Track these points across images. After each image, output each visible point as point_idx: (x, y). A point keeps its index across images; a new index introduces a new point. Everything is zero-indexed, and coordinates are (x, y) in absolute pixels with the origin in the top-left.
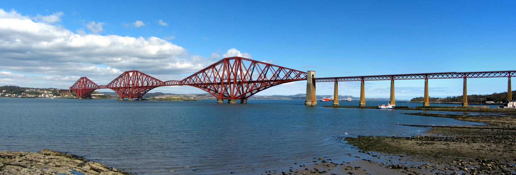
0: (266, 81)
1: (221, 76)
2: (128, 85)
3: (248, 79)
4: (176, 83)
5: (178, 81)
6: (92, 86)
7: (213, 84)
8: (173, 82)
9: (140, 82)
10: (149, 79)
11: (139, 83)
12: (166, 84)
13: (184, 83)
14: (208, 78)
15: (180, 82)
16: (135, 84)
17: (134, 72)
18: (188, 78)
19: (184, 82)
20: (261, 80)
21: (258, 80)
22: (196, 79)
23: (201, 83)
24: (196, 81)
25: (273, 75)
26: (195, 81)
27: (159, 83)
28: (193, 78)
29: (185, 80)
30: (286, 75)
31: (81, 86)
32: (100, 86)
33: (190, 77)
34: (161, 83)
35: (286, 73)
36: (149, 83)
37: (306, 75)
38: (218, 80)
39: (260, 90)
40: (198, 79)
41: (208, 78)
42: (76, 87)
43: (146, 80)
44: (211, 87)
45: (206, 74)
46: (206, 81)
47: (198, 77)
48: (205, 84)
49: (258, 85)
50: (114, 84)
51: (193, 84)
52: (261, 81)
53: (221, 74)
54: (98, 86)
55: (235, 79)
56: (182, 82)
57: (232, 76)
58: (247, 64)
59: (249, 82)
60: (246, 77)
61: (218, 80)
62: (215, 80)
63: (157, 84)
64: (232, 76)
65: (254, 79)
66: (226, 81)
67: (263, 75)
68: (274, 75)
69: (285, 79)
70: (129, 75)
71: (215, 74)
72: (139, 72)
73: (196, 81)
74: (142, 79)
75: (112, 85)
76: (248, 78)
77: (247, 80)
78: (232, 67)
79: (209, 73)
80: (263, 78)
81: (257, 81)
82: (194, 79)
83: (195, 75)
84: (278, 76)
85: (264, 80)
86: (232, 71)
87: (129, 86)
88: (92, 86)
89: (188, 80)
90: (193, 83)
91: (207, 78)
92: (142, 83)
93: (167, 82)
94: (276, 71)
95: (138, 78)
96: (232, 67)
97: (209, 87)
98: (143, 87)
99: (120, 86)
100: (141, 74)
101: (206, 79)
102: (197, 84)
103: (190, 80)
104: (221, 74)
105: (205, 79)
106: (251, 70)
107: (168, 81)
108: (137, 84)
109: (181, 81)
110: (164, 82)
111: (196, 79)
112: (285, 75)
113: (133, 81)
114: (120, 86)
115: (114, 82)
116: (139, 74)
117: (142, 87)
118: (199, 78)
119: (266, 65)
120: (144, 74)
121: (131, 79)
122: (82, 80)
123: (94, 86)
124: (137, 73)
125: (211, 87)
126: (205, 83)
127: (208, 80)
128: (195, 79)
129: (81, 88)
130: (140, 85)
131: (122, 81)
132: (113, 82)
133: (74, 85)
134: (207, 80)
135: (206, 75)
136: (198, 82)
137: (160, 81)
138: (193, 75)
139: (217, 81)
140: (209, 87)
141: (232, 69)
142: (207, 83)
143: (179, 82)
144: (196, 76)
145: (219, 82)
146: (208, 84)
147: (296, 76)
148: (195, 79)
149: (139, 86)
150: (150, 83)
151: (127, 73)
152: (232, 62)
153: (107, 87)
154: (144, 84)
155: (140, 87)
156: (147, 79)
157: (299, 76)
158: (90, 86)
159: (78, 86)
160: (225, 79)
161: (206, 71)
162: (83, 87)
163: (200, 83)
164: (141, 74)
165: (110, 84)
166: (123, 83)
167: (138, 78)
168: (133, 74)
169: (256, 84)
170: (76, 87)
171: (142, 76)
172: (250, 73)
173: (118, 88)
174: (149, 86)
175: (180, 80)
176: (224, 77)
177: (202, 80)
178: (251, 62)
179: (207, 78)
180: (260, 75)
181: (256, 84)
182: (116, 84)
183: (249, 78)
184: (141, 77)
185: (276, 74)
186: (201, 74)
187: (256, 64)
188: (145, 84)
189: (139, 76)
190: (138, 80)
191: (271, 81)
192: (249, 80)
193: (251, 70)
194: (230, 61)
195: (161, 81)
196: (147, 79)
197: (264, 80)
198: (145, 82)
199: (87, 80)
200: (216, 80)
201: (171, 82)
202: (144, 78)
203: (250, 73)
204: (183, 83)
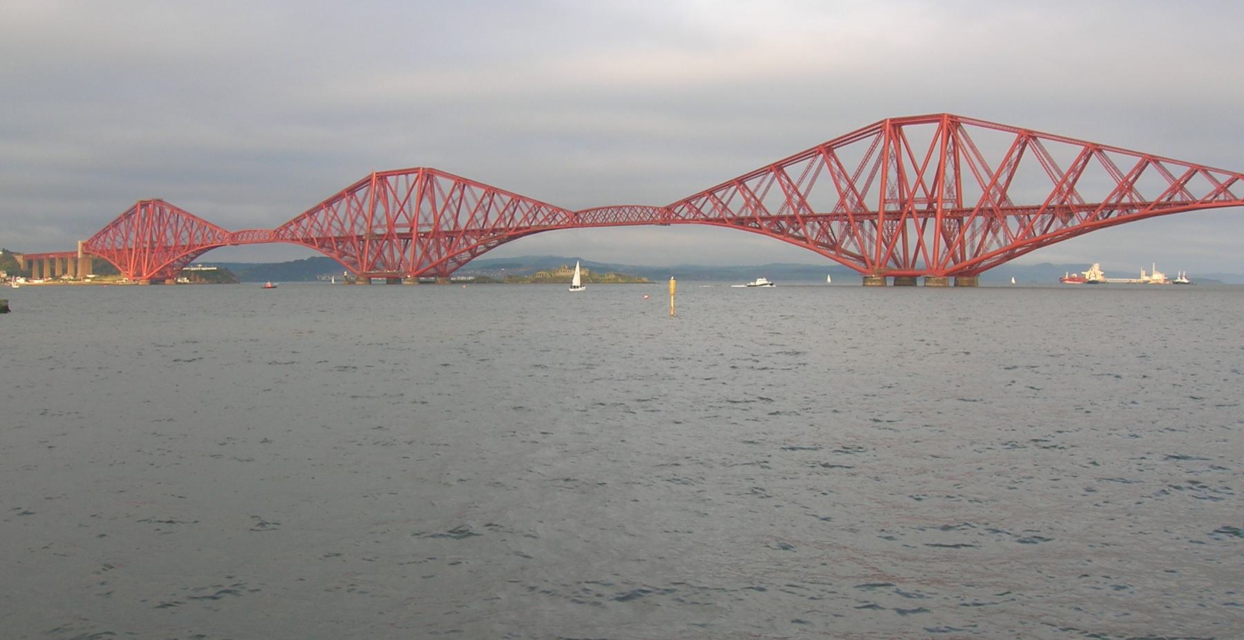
4: (265, 238)
8: (255, 235)
9: (169, 233)
10: (195, 226)
11: (168, 237)
13: (283, 236)
19: (282, 232)
20: (473, 228)
25: (498, 216)
28: (305, 222)
29: (286, 227)
30: (526, 217)
33: (298, 221)
35: (526, 213)
36: (195, 237)
37: (564, 216)
38: (362, 227)
39: (478, 251)
40: (316, 225)
43: (187, 229)
46: (333, 230)
50: (108, 240)
58: (446, 185)
60: (442, 220)
61: (362, 227)
62: (352, 230)
67: (479, 215)
68: (501, 218)
69: (522, 225)
71: (352, 211)
72: (170, 206)
74: (174, 227)
76: (447, 222)
77: (445, 229)
79: (342, 208)
80: (481, 223)
81: (466, 231)
84: (512, 218)
85: (485, 227)
89: (292, 228)
91: (336, 224)
92: (176, 236)
94: (507, 203)
97: (340, 247)
100: (172, 212)
104: (366, 208)
106: (454, 202)
107: (244, 232)
109: (275, 231)
112: (523, 216)
119: (484, 191)
125: (344, 246)
127: (340, 228)
136: (315, 234)
139: (359, 231)
142: (337, 235)
145: (362, 233)
147: (546, 218)
149: (169, 245)
150: (197, 238)
154: (181, 238)
155: (171, 247)
157: (554, 218)
161: (335, 205)
166: (133, 235)
171: (174, 215)
179: (336, 224)
180: (473, 216)
183: (452, 223)
184: (172, 221)
185: (507, 213)
187: (466, 187)
188: (186, 242)
189: (168, 214)
191: (494, 231)
192: (452, 229)
193: (454, 202)
196: (188, 224)
198: (185, 234)
200: (356, 228)
202: (181, 223)
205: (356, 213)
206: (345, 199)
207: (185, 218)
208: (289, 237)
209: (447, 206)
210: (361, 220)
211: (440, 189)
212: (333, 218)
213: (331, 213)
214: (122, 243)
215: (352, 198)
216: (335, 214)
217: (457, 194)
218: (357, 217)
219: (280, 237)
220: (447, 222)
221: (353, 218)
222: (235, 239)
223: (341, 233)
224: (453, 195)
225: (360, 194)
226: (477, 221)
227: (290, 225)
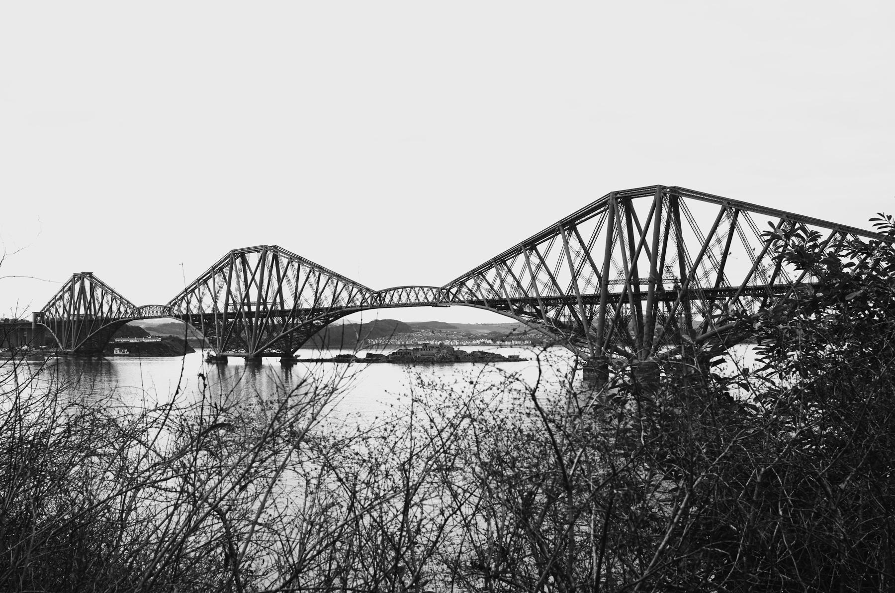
0: (781, 288)
1: (600, 265)
2: (243, 304)
3: (706, 280)
4: (426, 298)
5: (431, 288)
6: (115, 308)
7: (568, 300)
8: (412, 293)
12: (387, 300)
13: (455, 296)
14: (550, 274)
15: (440, 290)
16: (270, 300)
17: (263, 250)
18: (468, 276)
19: (454, 290)
20: (759, 283)
21: (750, 284)
22: (502, 281)
23: (523, 296)
24: (502, 286)
26: (496, 287)
27: (359, 296)
28: (491, 274)
29: (460, 283)
31: (75, 308)
32: (142, 308)
33: (478, 273)
34: (367, 295)
38: (588, 282)
40: (510, 279)
41: (550, 274)
42: (57, 311)
43: (311, 285)
44: (558, 314)
45: (540, 258)
46: (540, 287)
47: (510, 271)
48: (533, 302)
49: (748, 304)
51: (488, 301)
52: (760, 288)
53: (598, 255)
54: (138, 308)
55: (656, 278)
56: (449, 291)
57: (644, 269)
59: (710, 295)
60: (699, 272)
61: (588, 282)
63: (351, 299)
64: (644, 269)
65: (735, 277)
66: (618, 289)
70: (245, 262)
71: (573, 256)
72: (286, 253)
73: (502, 286)
75: (184, 305)
76: (706, 274)
77: (704, 284)
78: (643, 227)
79: (553, 250)
81: (744, 290)
82: (495, 281)
83: (500, 261)
85: (776, 282)
86: (643, 242)
87: (249, 308)
88: (115, 308)
90: (491, 297)
91: (543, 277)
92: (297, 297)
93: (387, 291)
95: (282, 274)
96: (643, 227)
97: (552, 314)
98: (299, 310)
99: (215, 308)
101: (541, 282)
102: (505, 301)
103: (478, 286)
104: (598, 255)
105: (534, 278)
106: (719, 241)
107: (394, 289)
108: (278, 300)
109: (443, 288)
110: (379, 294)
111: (502, 281)
113: (260, 288)
114: (215, 308)
115: (193, 291)
116: (284, 261)
117: (296, 312)
118: (513, 276)
120: (301, 260)
121: (253, 279)
122: (77, 287)
123: (119, 309)
124: (275, 258)
126: (535, 295)
127: (550, 283)
128: (498, 282)
129: (74, 315)
130: (289, 305)
131: (221, 287)
132: (189, 291)
133: (52, 304)
134: (546, 285)
135: (537, 261)
136: (510, 292)
137: (362, 289)
138: (489, 265)
140: (552, 314)
141: (643, 234)
142: (544, 295)
143: (434, 290)
144: (501, 267)
145: (591, 291)
146: (547, 301)
148: (495, 281)
149: (286, 308)
151: (242, 254)
152: (642, 206)
153: (167, 310)
155: (289, 311)
156: (312, 279)
158: (106, 308)
159: (64, 307)
160: (616, 282)
161: (542, 248)
162: (82, 311)
163: (517, 296)
164: (293, 258)
165: (176, 301)
167: (282, 274)
168: (263, 259)
169: (741, 298)
170: (57, 311)
172: (717, 251)
173: (208, 315)
174: (321, 309)
175: (440, 286)
176: (613, 275)
177: (526, 283)
178: (719, 207)
179: (543, 277)
181: (741, 298)
182: (200, 301)
183: (714, 277)
184: (291, 273)
186: (521, 258)
189: (285, 265)
190: (280, 281)
192: (713, 285)
193: (719, 241)
194: (636, 202)
195: (368, 290)
196: (312, 279)
197: (776, 282)
199: (95, 283)
200: (581, 283)
201: (404, 294)
203: (717, 251)
204: (451, 297)
205: (579, 259)
206: (560, 236)
207: (308, 270)
208: (466, 297)
209: (705, 249)
210: (587, 270)
211: (691, 221)
212: (538, 267)
213: (534, 260)
214: (212, 306)
215: (570, 235)
216: (542, 261)
217: (724, 227)
218: (581, 266)
219: (451, 297)
220: (706, 274)
221: (576, 266)
222: (378, 300)
223: (551, 289)
224: (718, 228)
225: (586, 229)
226: (764, 272)
227: (468, 279)
